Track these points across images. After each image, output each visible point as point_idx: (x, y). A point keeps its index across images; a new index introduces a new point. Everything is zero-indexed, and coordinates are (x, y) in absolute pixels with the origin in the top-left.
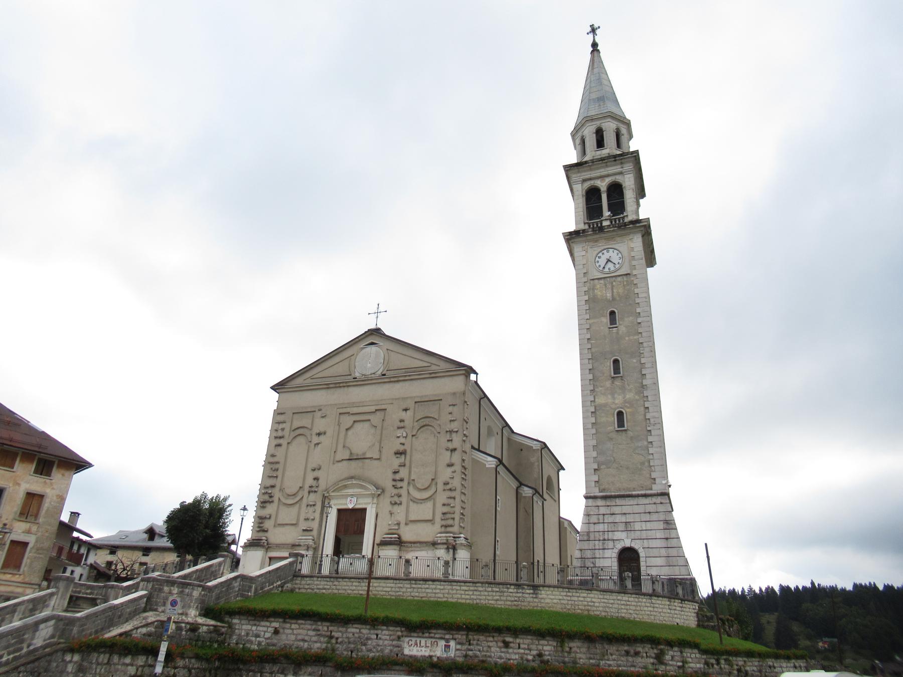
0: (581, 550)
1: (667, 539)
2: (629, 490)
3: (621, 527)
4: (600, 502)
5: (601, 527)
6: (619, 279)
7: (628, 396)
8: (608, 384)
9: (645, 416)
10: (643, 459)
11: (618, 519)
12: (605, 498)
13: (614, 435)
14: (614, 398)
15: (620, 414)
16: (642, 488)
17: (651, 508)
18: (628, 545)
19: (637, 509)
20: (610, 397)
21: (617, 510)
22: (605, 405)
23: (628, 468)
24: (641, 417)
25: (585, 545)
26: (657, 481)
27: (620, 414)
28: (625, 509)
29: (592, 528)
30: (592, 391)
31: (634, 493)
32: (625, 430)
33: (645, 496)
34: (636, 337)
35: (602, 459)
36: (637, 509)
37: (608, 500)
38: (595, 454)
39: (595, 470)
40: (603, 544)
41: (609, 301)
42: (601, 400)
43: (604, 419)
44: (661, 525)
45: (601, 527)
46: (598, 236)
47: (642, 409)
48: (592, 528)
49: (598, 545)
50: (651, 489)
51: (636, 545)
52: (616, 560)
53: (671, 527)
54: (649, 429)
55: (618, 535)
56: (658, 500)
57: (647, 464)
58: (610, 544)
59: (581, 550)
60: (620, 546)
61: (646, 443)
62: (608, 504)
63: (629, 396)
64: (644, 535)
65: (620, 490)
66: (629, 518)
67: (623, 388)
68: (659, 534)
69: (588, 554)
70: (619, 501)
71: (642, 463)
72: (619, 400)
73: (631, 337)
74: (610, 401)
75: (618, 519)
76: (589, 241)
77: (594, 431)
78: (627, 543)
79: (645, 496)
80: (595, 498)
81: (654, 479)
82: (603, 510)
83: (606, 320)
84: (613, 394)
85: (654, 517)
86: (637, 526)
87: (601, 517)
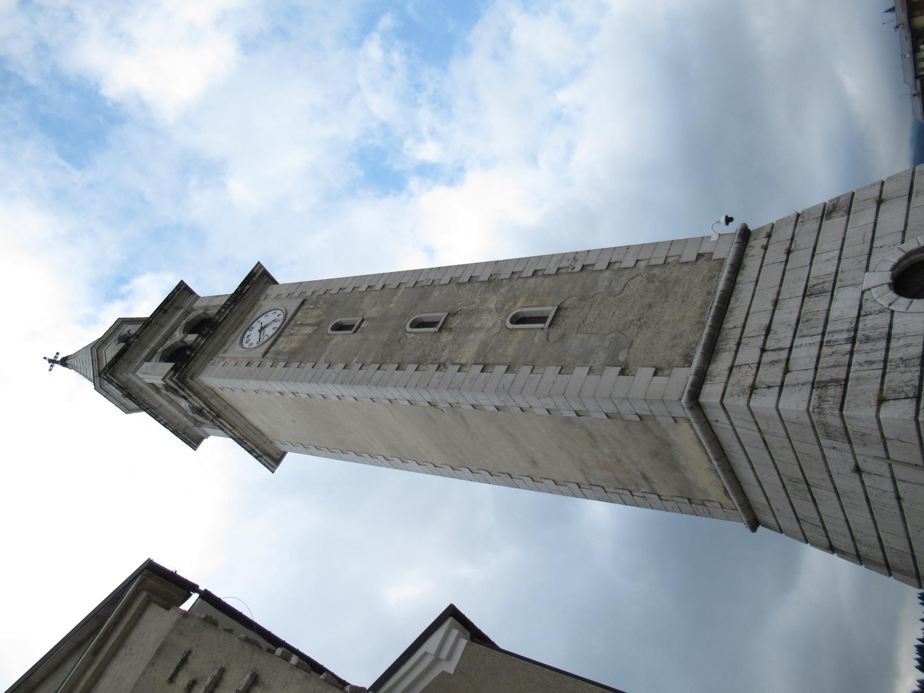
0: (881, 401)
2: (706, 303)
3: (817, 305)
4: (721, 365)
5: (804, 355)
6: (299, 314)
7: (492, 306)
8: (445, 337)
9: (549, 275)
10: (640, 278)
12: (711, 351)
13: (556, 333)
14: (479, 330)
15: (518, 320)
17: (776, 252)
18: (887, 277)
19: (771, 276)
20: (472, 336)
22: (485, 344)
23: (650, 306)
24: (548, 282)
26: (705, 249)
27: (518, 320)
28: (763, 302)
30: (441, 367)
31: (721, 285)
32: (559, 309)
33: (737, 267)
34: (400, 292)
35: (601, 356)
36: (771, 276)
37: (720, 345)
38: (581, 372)
39: (622, 373)
40: (868, 339)
41: (314, 332)
42: (468, 353)
43: (511, 350)
45: (804, 355)
46: (218, 338)
47: (532, 281)
50: (722, 261)
51: (888, 258)
54: (578, 268)
55: (845, 304)
56: (756, 246)
57: (655, 271)
58: (874, 323)
59: (881, 401)
61: (607, 274)
62: (732, 345)
63: (493, 301)
65: (701, 324)
67: (470, 314)
70: (734, 320)
71: (650, 279)
72: (489, 321)
73: (396, 298)
74: (481, 336)
75: (787, 313)
76: (214, 353)
77: (526, 370)
79: (737, 267)
81: (699, 256)
82: (749, 354)
83: (340, 335)
84: (471, 330)
85: (805, 240)
86: (824, 268)
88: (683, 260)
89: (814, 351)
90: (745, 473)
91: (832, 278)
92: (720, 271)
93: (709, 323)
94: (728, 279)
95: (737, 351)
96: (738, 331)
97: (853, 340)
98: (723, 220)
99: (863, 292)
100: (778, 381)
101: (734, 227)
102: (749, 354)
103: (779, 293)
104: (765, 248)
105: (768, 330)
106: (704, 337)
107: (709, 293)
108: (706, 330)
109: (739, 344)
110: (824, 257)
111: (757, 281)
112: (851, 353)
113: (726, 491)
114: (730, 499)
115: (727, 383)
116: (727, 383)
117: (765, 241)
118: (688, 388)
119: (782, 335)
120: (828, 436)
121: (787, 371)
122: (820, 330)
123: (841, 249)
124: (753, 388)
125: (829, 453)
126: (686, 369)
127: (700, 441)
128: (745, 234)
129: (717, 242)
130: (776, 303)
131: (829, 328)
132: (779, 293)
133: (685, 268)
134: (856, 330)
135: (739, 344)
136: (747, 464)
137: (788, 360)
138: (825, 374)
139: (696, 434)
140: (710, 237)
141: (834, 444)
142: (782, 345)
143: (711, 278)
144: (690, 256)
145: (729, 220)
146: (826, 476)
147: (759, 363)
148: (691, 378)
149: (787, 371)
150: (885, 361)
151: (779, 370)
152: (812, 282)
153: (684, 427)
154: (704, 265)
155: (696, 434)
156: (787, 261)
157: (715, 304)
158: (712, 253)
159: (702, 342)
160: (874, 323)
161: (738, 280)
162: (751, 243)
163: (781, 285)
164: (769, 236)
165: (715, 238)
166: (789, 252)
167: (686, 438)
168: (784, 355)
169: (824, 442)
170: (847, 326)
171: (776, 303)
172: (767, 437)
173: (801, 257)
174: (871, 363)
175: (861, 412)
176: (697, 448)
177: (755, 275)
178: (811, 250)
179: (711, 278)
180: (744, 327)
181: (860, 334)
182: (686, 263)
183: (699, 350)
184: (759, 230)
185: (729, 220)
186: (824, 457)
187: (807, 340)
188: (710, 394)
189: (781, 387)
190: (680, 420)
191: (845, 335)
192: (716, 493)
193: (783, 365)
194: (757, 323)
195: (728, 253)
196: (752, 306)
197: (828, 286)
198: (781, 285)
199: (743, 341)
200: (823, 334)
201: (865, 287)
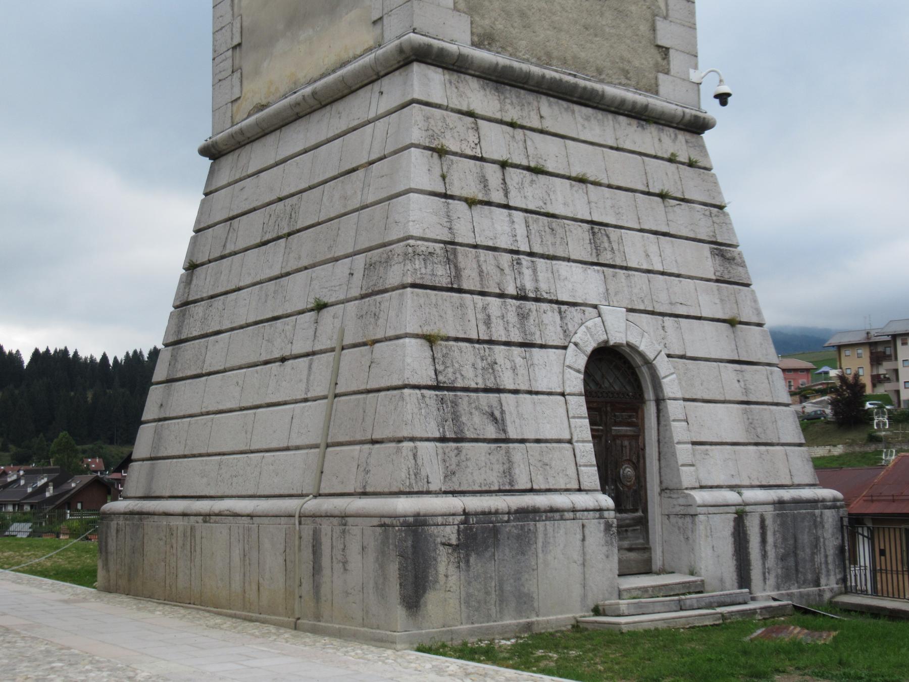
0: (430, 340)
1: (732, 323)
2: (580, 66)
3: (578, 242)
4: (478, 97)
5: (497, 227)
11: (564, 199)
12: (500, 79)
16: (626, 76)
17: (664, 177)
18: (617, 337)
19: (625, 170)
21: (548, 152)
25: (449, 315)
26: (676, 60)
28: (582, 160)
29: (471, 225)
31: (613, 91)
33: (642, 116)
36: (625, 170)
37: (511, 94)
40: (523, 317)
44: (703, 262)
45: (497, 227)
48: (471, 225)
49: (503, 320)
50: (654, 90)
52: (579, 405)
53: (736, 273)
58: (548, 325)
59: (430, 340)
60: (588, 338)
62: (512, 114)
64: (664, 294)
66: (602, 206)
68: (709, 301)
69: (466, 366)
70: (555, 115)
75: (564, 199)
78: (619, 329)
80: (454, 65)
81: (664, 51)
82: (496, 142)
85: (681, 219)
86: (635, 249)
87: (493, 173)
88: (660, 24)
89: (503, 243)
90: (296, 138)
91: (618, 262)
92: (637, 88)
93: (549, 74)
94: (623, 102)
95: (501, 122)
96: (536, 124)
97: (522, 297)
98: (724, 89)
99: (595, 307)
100: (455, 191)
101: (710, 108)
102: (496, 142)
103: (596, 184)
104: (672, 160)
105: (537, 171)
106: (525, 67)
107: (600, 71)
108: (536, 70)
109: (512, 125)
110: (653, 249)
111: (617, 149)
112: (502, 295)
113: (263, 107)
114: (249, 115)
115: (447, 108)
116: (447, 108)
117: (683, 158)
118: (436, 43)
119: (528, 192)
120: (370, 266)
121: (471, 202)
122: (537, 249)
123: (663, 273)
124: (441, 152)
125: (343, 267)
126: (467, 38)
127: (343, 65)
128: (697, 126)
129: (686, 80)
130: (582, 180)
131: (540, 262)
132: (596, 184)
133: (644, 28)
134: (537, 300)
135: (512, 125)
136: (312, 142)
137: (489, 203)
138: (466, 259)
139: (355, 58)
140: (696, 67)
141: (358, 275)
142: (513, 193)
143: (626, 73)
144: (666, 34)
145: (723, 98)
146: (305, 262)
147: (482, 159)
148: (453, 48)
149: (471, 202)
150: (491, 342)
151: (473, 190)
152: (614, 233)
153: (367, 37)
154: (647, 59)
155: (355, 58)
156: (649, 194)
157: (582, 83)
158: (667, 72)
159: (516, 65)
160: (548, 325)
161: (622, 119)
162: (682, 137)
163: (610, 186)
164: (691, 164)
165: (694, 76)
166: (663, 196)
167: (345, 42)
168: (497, 196)
169: (360, 259)
170: (543, 286)
171: (582, 180)
172: (360, 173)
173: (655, 215)
174: (488, 322)
175: (411, 312)
176: (330, 59)
177: (628, 145)
178: (664, 229)
179: (626, 73)
180: (542, 132)
181: (532, 305)
182: (654, 29)
183: (502, 60)
184: (702, 148)
185: (723, 98)
186: (336, 260)
187: (521, 230)
188: (428, 82)
189: (445, 196)
190: (378, 30)
191: (529, 285)
192: (256, 90)
193: (480, 197)
194: (548, 152)
195: (668, 98)
196: (578, 142)
197: (606, 258)
198: (610, 186)
199: (519, 132)
200: (531, 254)
201: (604, 309)
